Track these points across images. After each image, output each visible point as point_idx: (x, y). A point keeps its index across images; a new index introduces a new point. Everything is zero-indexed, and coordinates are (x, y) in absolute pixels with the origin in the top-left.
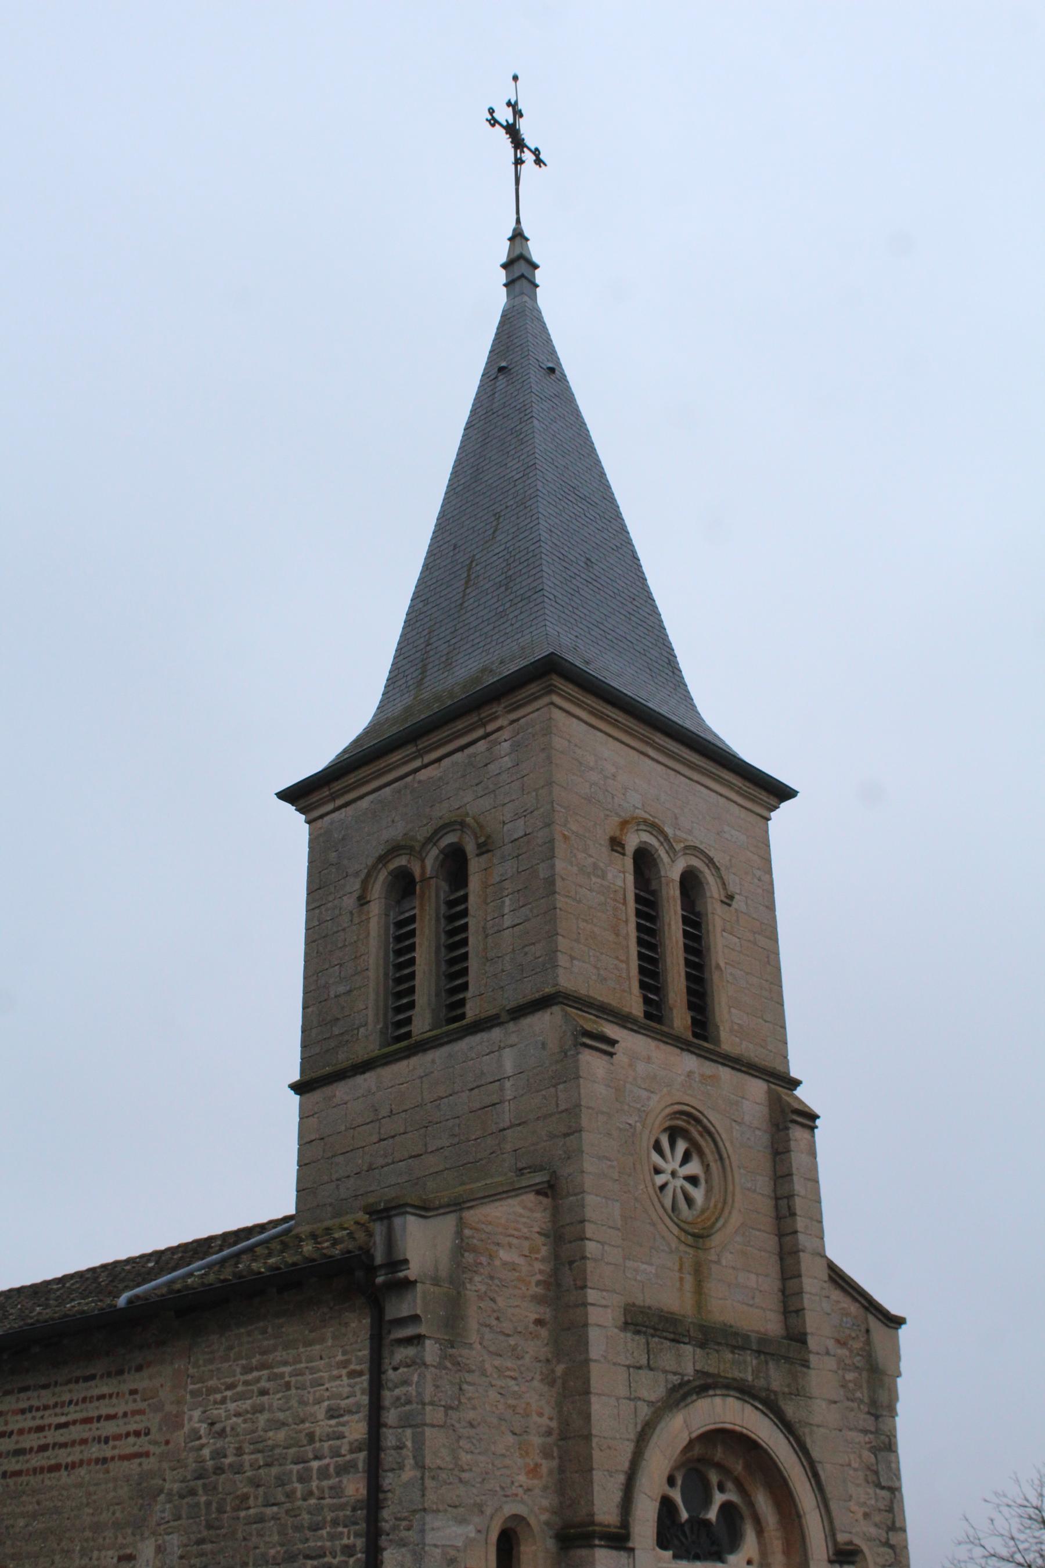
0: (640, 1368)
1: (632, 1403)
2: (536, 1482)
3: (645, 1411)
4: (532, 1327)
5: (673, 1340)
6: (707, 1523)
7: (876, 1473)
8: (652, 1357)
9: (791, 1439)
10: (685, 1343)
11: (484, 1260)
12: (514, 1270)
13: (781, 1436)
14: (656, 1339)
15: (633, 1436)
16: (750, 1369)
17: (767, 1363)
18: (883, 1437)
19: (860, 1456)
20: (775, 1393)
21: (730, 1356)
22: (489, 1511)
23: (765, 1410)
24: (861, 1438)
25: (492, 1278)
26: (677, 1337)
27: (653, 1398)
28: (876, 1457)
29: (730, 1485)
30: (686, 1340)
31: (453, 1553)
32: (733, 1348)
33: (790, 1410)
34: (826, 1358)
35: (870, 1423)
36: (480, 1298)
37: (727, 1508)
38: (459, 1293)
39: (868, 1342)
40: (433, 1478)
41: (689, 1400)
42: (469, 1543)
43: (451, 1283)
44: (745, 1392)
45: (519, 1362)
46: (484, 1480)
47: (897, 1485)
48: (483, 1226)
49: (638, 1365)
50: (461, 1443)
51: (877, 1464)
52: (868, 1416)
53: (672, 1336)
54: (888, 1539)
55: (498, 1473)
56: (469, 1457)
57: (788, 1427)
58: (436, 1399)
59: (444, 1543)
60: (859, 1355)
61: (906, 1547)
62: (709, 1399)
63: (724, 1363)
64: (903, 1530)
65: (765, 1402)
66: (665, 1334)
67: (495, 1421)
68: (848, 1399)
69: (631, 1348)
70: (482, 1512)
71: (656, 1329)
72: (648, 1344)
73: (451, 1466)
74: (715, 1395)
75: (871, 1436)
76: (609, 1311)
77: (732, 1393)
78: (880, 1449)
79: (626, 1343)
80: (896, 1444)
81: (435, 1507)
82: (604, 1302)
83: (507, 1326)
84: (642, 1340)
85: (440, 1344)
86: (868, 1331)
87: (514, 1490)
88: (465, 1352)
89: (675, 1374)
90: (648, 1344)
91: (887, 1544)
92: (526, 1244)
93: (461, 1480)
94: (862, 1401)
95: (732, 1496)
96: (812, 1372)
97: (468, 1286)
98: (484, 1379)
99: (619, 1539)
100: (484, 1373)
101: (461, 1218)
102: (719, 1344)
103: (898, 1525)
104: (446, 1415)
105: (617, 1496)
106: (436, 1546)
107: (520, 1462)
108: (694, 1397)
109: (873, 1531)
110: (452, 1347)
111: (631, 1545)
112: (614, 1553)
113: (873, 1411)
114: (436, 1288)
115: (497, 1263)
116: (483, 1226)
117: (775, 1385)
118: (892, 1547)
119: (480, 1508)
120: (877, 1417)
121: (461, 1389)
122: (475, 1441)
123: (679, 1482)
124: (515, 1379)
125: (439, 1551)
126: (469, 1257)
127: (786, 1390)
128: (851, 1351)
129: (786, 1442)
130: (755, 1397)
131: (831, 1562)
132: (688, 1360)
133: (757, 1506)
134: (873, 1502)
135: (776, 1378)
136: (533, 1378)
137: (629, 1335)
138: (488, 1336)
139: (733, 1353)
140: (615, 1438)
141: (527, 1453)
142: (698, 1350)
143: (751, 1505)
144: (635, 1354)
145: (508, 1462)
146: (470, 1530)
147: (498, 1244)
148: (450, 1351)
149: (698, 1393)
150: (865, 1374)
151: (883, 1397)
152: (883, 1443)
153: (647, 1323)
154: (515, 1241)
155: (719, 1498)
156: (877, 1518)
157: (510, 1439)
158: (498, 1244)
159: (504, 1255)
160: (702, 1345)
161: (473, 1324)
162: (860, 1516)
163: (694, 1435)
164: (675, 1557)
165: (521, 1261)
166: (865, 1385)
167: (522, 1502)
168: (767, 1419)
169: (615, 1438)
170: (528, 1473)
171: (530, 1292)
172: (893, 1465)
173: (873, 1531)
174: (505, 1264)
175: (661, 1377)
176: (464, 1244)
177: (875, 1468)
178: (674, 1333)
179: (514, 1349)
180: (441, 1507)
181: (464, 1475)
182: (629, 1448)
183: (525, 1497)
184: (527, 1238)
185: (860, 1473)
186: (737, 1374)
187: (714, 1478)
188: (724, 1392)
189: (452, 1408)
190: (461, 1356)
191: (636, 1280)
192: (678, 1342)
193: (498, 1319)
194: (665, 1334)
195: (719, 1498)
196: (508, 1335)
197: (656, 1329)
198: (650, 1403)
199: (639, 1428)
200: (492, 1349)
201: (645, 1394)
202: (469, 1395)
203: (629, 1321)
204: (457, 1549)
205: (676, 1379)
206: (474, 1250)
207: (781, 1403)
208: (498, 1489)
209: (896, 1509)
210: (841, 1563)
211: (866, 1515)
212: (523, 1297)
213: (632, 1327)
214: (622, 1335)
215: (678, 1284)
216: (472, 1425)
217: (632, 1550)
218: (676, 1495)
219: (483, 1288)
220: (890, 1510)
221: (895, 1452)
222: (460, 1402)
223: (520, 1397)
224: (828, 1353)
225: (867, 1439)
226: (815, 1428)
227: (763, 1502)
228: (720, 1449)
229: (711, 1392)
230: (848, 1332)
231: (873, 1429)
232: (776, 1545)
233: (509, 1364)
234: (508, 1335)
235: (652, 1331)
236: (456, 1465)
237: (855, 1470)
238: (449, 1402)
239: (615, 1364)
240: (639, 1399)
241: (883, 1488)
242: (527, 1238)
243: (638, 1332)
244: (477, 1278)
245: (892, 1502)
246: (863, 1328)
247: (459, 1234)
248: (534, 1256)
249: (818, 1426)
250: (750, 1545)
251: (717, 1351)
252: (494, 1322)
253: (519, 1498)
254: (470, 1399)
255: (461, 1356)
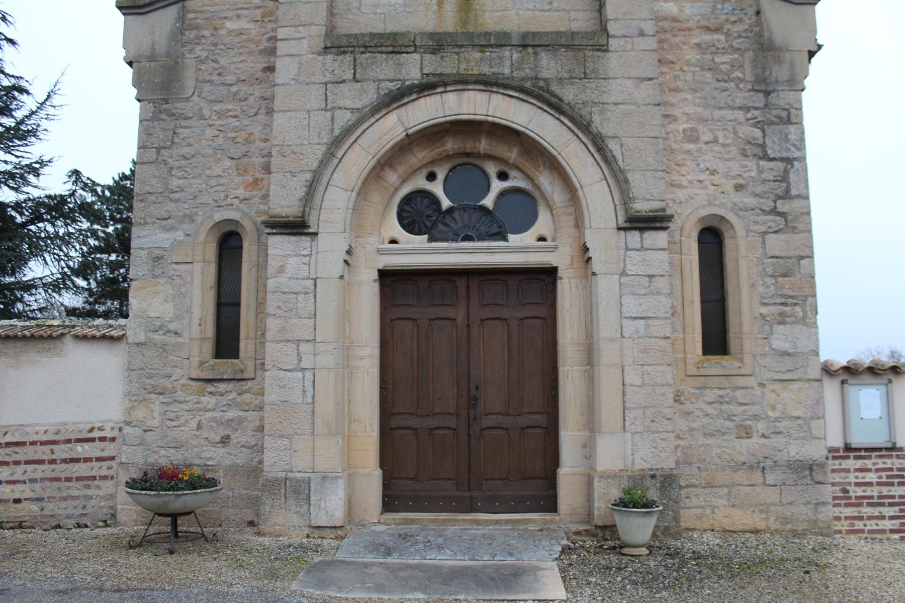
0: (343, 82)
1: (329, 114)
2: (255, 193)
3: (344, 118)
4: (259, 74)
5: (392, 52)
6: (483, 209)
7: (763, 146)
8: (358, 71)
9: (566, 121)
10: (407, 53)
11: (206, 33)
12: (241, 34)
13: (550, 118)
14: (368, 55)
15: (326, 139)
16: (507, 63)
17: (535, 54)
18: (775, 112)
19: (735, 132)
20: (546, 80)
21: (478, 55)
22: (199, 219)
23: (521, 96)
24: (740, 115)
25: (215, 45)
26: (398, 49)
27: (359, 105)
28: (763, 132)
29: (513, 173)
30: (412, 49)
31: (159, 252)
32: (482, 48)
33: (569, 94)
34: (640, 39)
35: (759, 100)
36: (202, 62)
37: (503, 194)
38: (176, 63)
39: (759, 23)
40: (142, 201)
41: (406, 100)
42: (177, 244)
43: (168, 56)
44: (489, 83)
45: (243, 103)
46: (195, 197)
47: (797, 154)
48: (209, 8)
49: (340, 80)
50: (173, 173)
51: (764, 138)
52: (752, 93)
53: (390, 49)
54: (775, 207)
55: (212, 190)
56: (181, 182)
57: (556, 106)
58: (148, 143)
59: (150, 246)
60: (740, 36)
61: (809, 213)
62: (438, 96)
63: (473, 62)
64: (807, 198)
65: (521, 90)
66: (380, 49)
67: (210, 151)
68: (718, 80)
69: (341, 66)
70: (193, 221)
71: (366, 47)
72: (355, 60)
73: (162, 190)
74: (445, 92)
75: (756, 113)
76: (305, 41)
77: (470, 87)
78: (772, 123)
79: (324, 65)
80: (800, 116)
81: (142, 221)
82: (299, 35)
83: (230, 79)
84: (348, 58)
85: (154, 103)
86: (758, 13)
87: (229, 201)
88: (181, 105)
89: (391, 81)
90: (355, 60)
91: (774, 212)
92: (258, 12)
93: (171, 200)
94: (741, 80)
95: (516, 181)
96: (610, 55)
97: (187, 55)
98: (202, 122)
99: (296, 227)
100: (202, 118)
101: (183, 7)
102: (461, 46)
103: (794, 192)
104: (158, 153)
105: (301, 192)
106: (141, 249)
107: (238, 179)
108: (414, 96)
109: (751, 201)
110: (167, 103)
111: (311, 230)
112: (293, 238)
113: (763, 87)
114: (152, 64)
115: (223, 32)
116: (209, 8)
117: (545, 74)
118: (782, 215)
119: (191, 218)
120: (767, 93)
121: (174, 133)
122: (187, 169)
123: (441, 177)
124: (236, 117)
125: (146, 252)
126: (192, 34)
127: (566, 75)
128: (728, 34)
129: (557, 122)
130: (506, 87)
131: (619, 229)
132: (413, 68)
133: (541, 187)
134: (753, 174)
135: (549, 66)
136: (256, 114)
137: (329, 57)
138: (207, 88)
139: (483, 52)
140: (302, 144)
141: (245, 171)
142: (428, 57)
143: (538, 188)
144: (336, 72)
145: (222, 181)
146: (179, 235)
147: (225, 18)
148: (165, 106)
149: (419, 92)
150: (749, 55)
151: (780, 73)
152: (779, 117)
153: (355, 43)
154: (244, 12)
155: (497, 186)
156: (759, 189)
157: (228, 163)
158: (225, 18)
159: (229, 25)
160: (434, 52)
161: (190, 83)
162: (728, 186)
163: (410, 131)
164: (431, 240)
165: (252, 26)
166: (748, 66)
167: (238, 209)
168: (526, 105)
169: (302, 144)
170: (245, 188)
171: (261, 47)
172: (792, 137)
173: (751, 201)
174: (230, 32)
175: (373, 86)
176: (185, 26)
177: (761, 141)
178: (392, 46)
179: (235, 94)
180: (149, 220)
181: (173, 196)
182: (320, 151)
183: (242, 206)
184: (259, 7)
185: (732, 148)
186: (486, 70)
187: (492, 169)
188: (459, 87)
189: (164, 148)
190: (176, 108)
191: (376, 13)
192: (400, 53)
193: (219, 74)
194: (380, 49)
195: (497, 186)
196: (231, 85)
197: (366, 47)
198: (352, 110)
199: (337, 132)
200: (212, 98)
201: (349, 104)
202: (181, 137)
203: (329, 45)
204: (165, 250)
205: (392, 86)
206: (197, 27)
207: (554, 88)
208: (211, 202)
209: (792, 177)
210: (642, 230)
211: (738, 188)
212: (250, 53)
213: (335, 50)
214: (320, 58)
215: (435, 8)
216: (185, 158)
217: (316, 234)
218: (437, 188)
219: (204, 54)
220: (784, 178)
221: (800, 123)
222: (173, 142)
223: (242, 130)
224: (642, 34)
225: (749, 115)
226: (611, 107)
227: (546, 181)
228: (483, 141)
229: (439, 90)
230: (724, 17)
231: (761, 105)
232: (568, 221)
233: (231, 107)
234: (231, 85)
235: (363, 49)
236: (166, 188)
237: (724, 146)
238: (162, 144)
239: (307, 84)
240: (340, 108)
241: (773, 159)
242: (259, 7)
243: (344, 52)
244: (198, 48)
245: (786, 171)
246: (751, 11)
247: (181, 18)
248: (266, 20)
249: (616, 104)
250: (543, 224)
251: (458, 54)
252: (215, 78)
253: (235, 207)
254: (183, 139)
255: (176, 108)
